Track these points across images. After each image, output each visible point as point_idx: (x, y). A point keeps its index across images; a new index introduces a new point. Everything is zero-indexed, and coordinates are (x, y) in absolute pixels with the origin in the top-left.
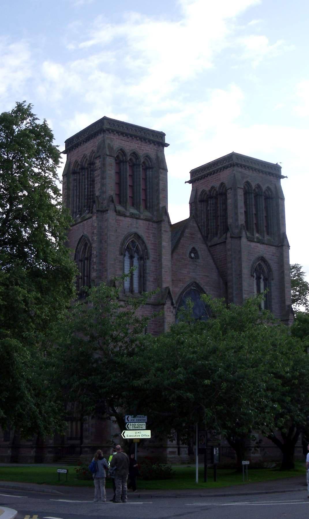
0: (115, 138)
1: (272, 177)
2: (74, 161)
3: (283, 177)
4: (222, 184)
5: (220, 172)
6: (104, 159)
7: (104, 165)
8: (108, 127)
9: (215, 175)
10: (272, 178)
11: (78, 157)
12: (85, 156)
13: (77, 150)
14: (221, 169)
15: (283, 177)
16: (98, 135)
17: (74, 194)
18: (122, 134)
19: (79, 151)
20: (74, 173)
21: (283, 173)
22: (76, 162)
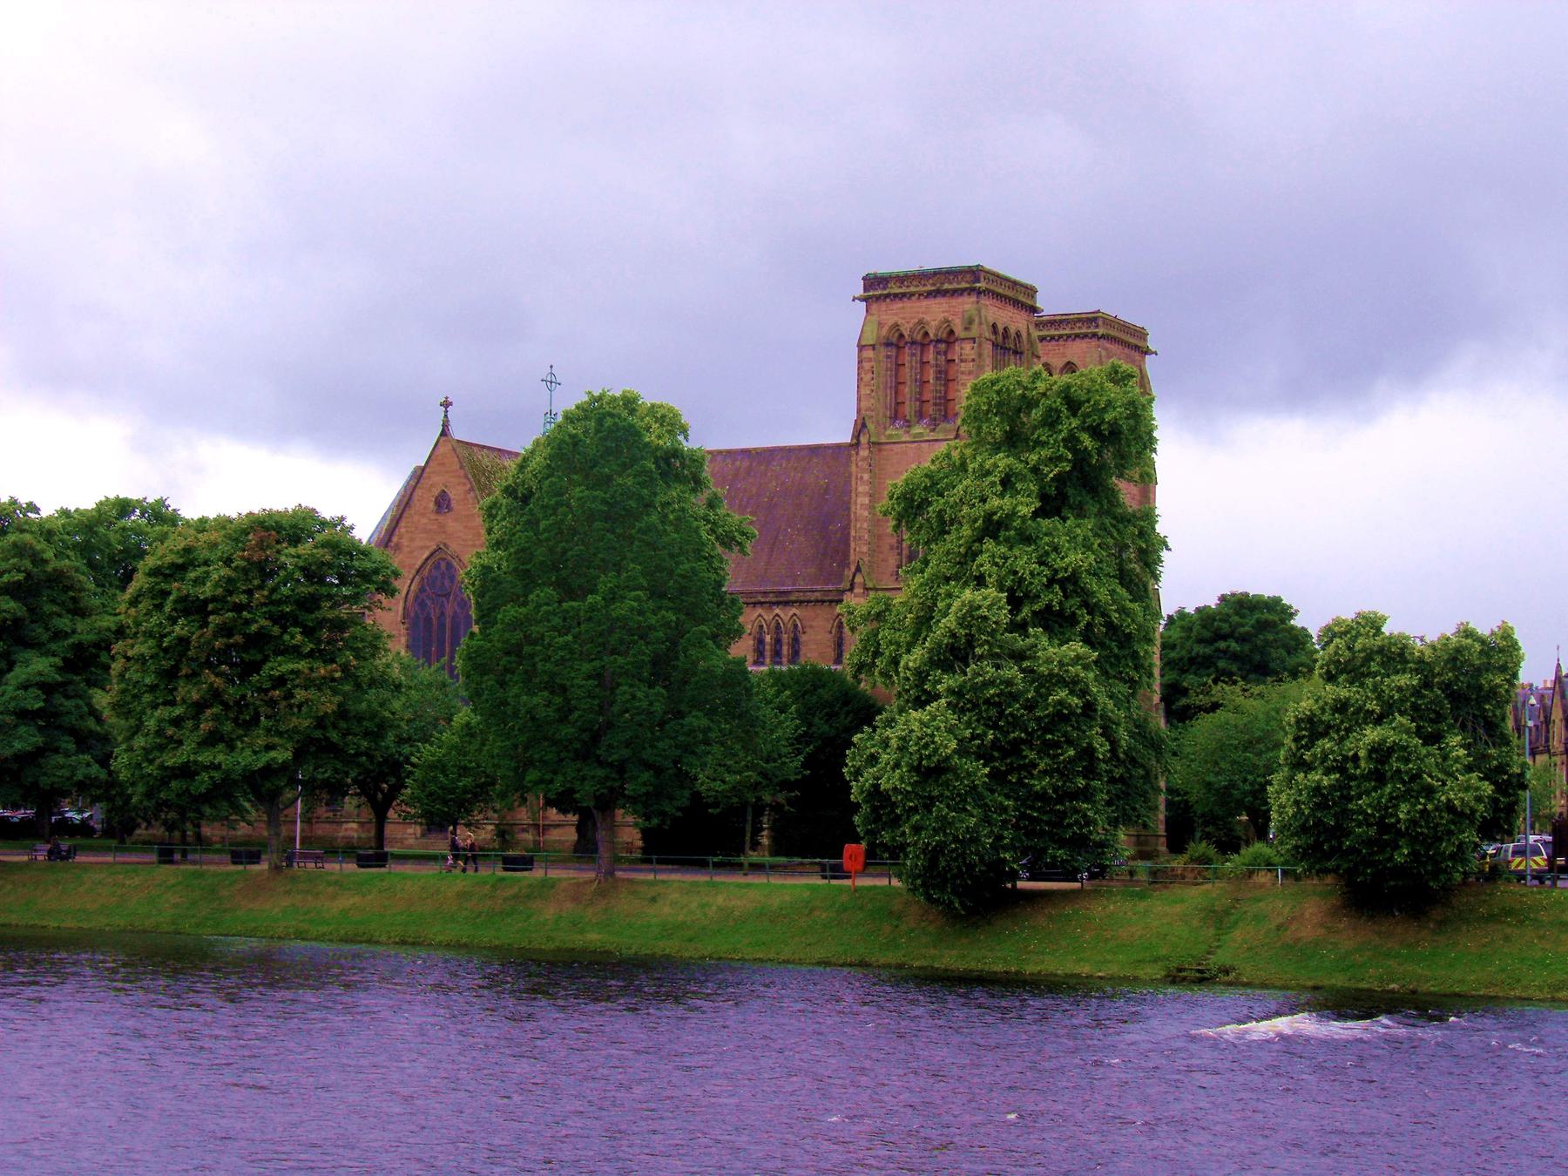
0: (988, 303)
1: (1137, 354)
2: (891, 322)
3: (1147, 352)
4: (1069, 363)
5: (1066, 340)
6: (980, 345)
7: (980, 355)
8: (982, 285)
9: (1053, 343)
10: (1137, 355)
11: (904, 318)
12: (920, 322)
13: (898, 305)
14: (1069, 336)
15: (1147, 352)
16: (961, 294)
17: (887, 383)
18: (998, 296)
19: (903, 308)
20: (888, 344)
21: (1151, 346)
22: (896, 325)
